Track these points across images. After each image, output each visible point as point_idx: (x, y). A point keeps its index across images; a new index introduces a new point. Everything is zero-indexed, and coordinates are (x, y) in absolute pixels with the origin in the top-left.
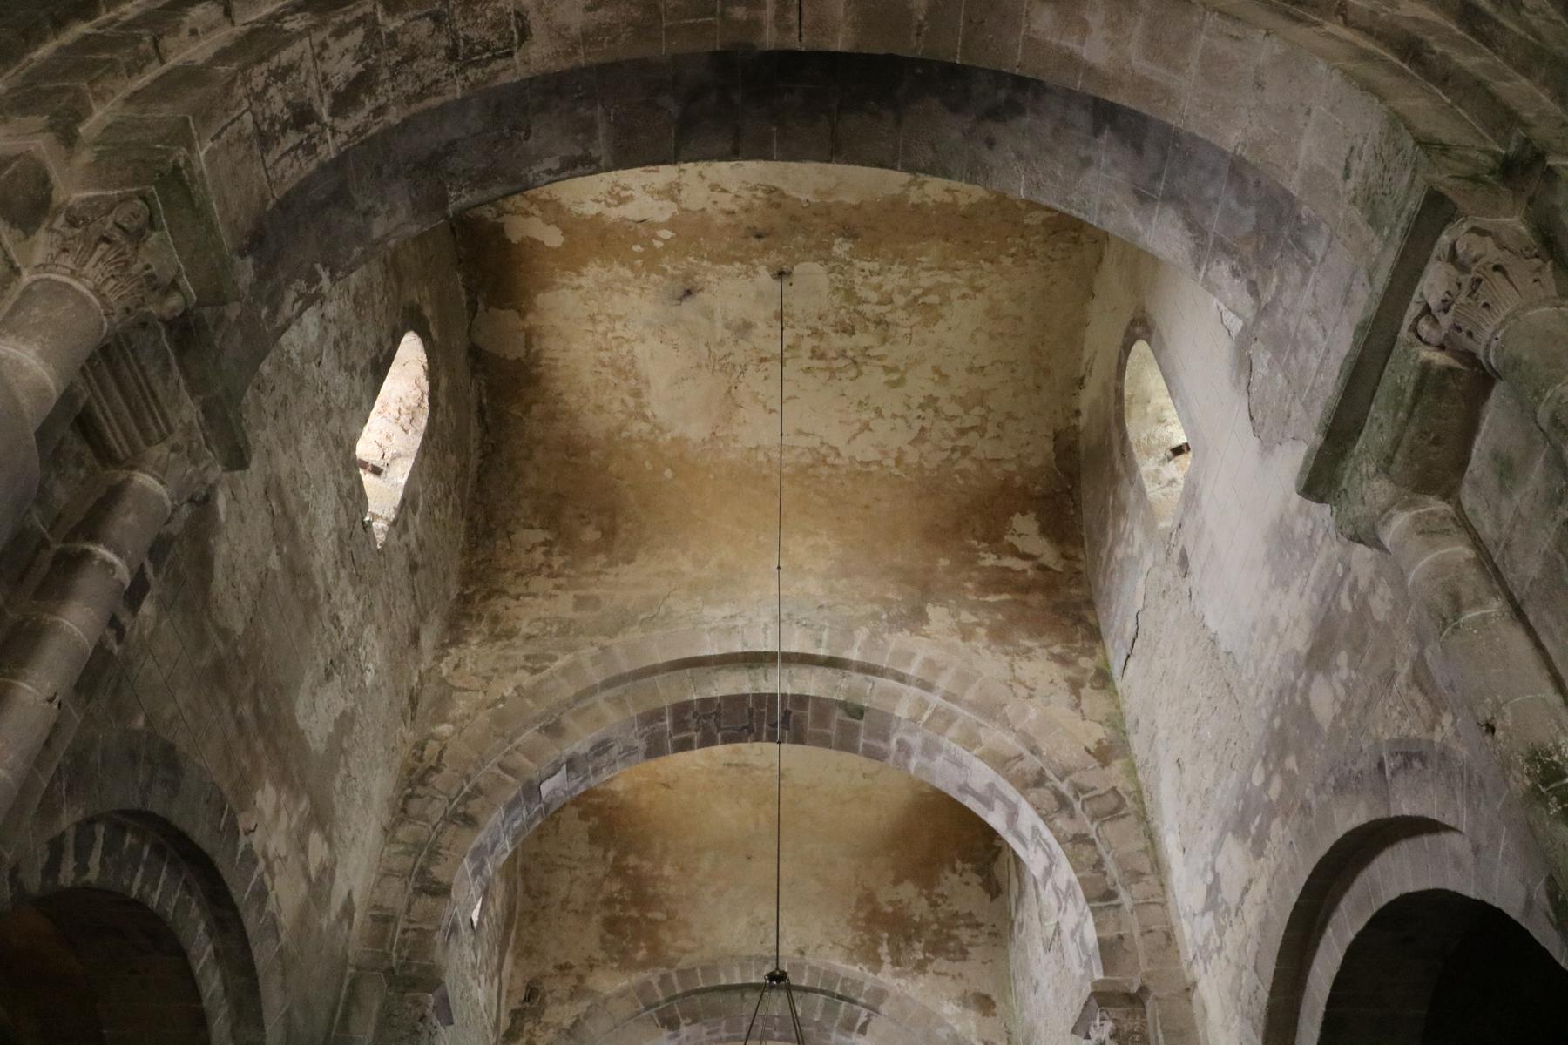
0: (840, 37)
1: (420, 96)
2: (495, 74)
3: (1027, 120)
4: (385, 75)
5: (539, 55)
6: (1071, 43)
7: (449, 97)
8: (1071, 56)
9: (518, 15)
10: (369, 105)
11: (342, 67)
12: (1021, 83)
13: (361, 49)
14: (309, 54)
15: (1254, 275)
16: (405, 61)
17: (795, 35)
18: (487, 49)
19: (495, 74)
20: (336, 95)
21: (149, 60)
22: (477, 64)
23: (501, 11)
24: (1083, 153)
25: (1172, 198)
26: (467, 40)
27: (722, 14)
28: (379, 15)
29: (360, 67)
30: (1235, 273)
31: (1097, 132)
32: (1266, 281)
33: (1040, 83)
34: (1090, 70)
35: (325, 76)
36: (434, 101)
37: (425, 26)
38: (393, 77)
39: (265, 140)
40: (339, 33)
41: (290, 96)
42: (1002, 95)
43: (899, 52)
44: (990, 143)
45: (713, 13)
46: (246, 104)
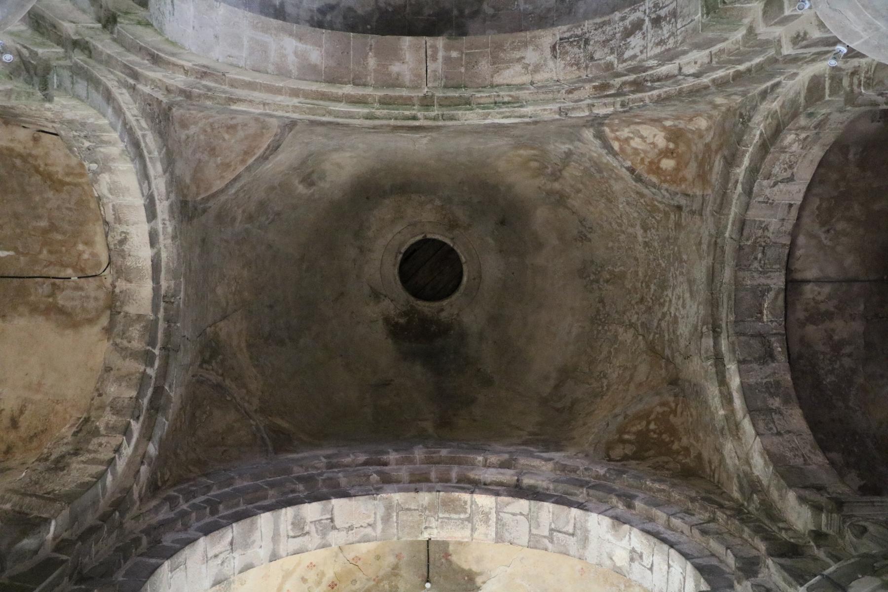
0: (407, 44)
1: (604, 23)
2: (568, 30)
4: (618, 35)
5: (548, 37)
6: (301, 46)
7: (591, 22)
8: (300, 39)
9: (556, 57)
10: (627, 22)
11: (636, 41)
12: (320, 25)
13: (626, 49)
14: (649, 49)
16: (608, 41)
17: (428, 44)
18: (571, 42)
19: (568, 30)
20: (641, 29)
21: (715, 54)
22: (577, 36)
23: (563, 59)
26: (580, 47)
27: (462, 53)
28: (616, 62)
29: (628, 40)
33: (312, 26)
34: (291, 34)
35: (644, 39)
36: (598, 20)
37: (596, 56)
38: (615, 34)
39: (674, 14)
40: (634, 57)
41: (660, 32)
42: (328, 18)
43: (380, 37)
45: (466, 54)
46: (679, 32)
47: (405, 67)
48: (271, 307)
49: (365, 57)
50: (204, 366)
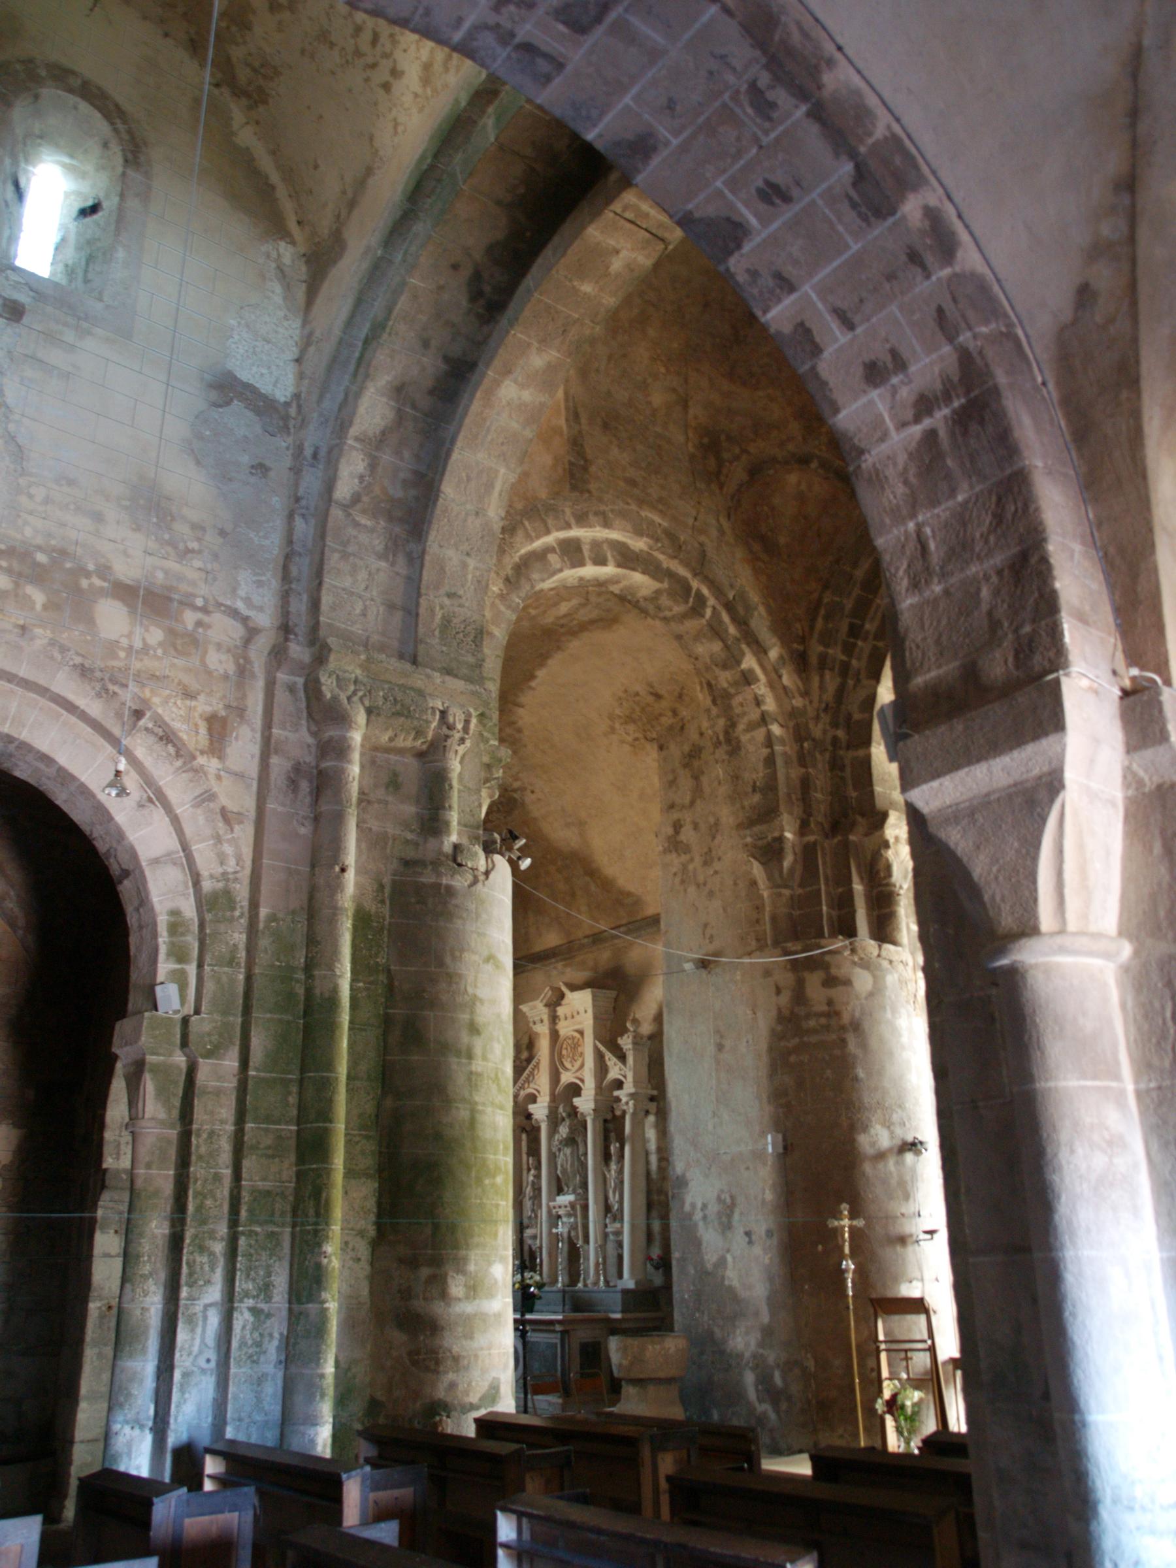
3: (464, 303)
8: (510, 372)
15: (365, 499)
17: (619, 211)
24: (434, 343)
25: (400, 417)
30: (361, 478)
31: (446, 359)
32: (364, 512)
34: (497, 383)
44: (455, 267)
47: (624, 254)
48: (706, 305)
49: (575, 291)
50: (722, 478)
